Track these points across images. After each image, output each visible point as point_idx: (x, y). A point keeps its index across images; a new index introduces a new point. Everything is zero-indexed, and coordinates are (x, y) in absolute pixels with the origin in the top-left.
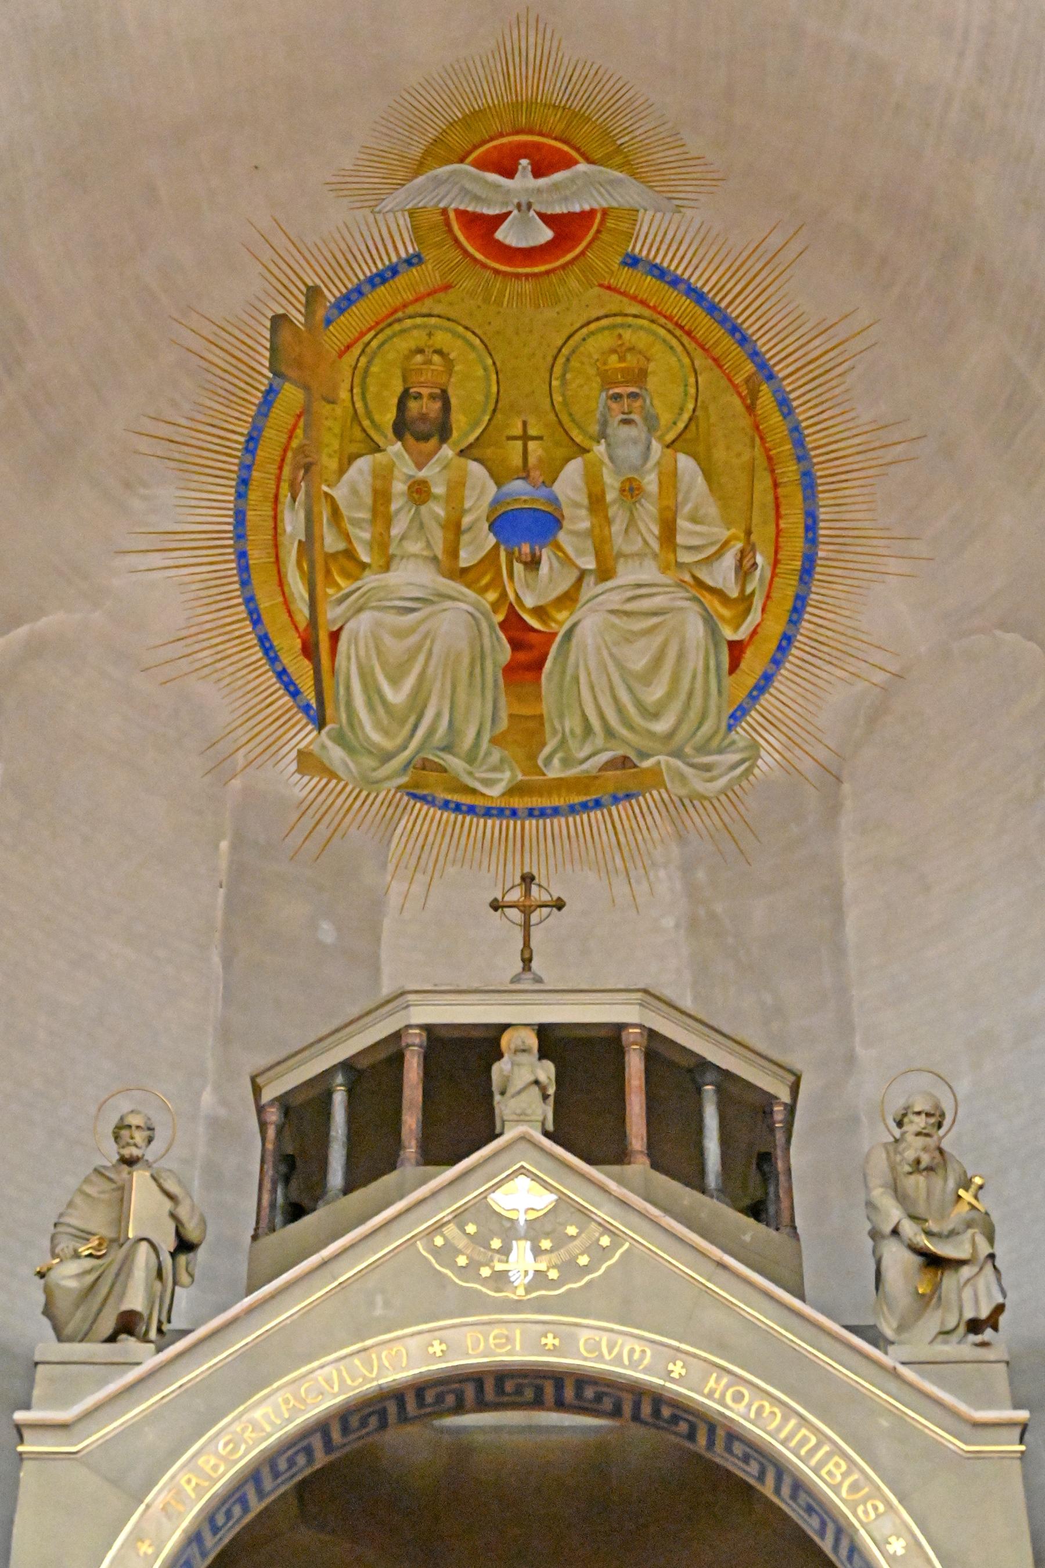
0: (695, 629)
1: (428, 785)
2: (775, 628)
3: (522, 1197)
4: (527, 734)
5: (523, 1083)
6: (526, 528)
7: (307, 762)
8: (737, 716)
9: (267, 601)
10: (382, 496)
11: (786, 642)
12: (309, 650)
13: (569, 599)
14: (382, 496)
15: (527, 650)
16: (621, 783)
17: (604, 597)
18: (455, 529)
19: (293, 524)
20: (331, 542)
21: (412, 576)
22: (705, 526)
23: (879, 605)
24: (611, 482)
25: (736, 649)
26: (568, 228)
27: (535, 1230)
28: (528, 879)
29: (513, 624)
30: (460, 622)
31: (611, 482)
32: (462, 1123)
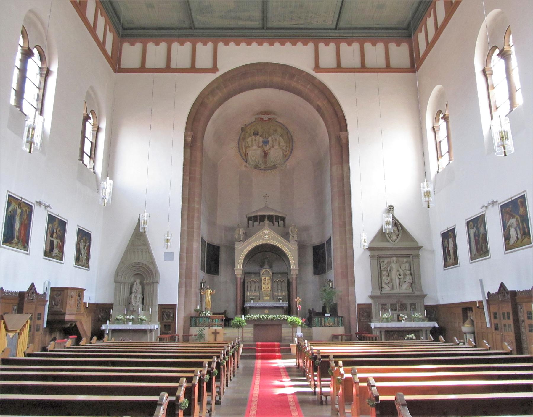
0: (282, 153)
2: (289, 154)
3: (266, 231)
4: (265, 162)
5: (266, 221)
6: (266, 143)
7: (245, 166)
8: (285, 162)
9: (241, 151)
10: (252, 140)
11: (290, 156)
12: (245, 155)
13: (270, 149)
14: (252, 140)
15: (266, 154)
17: (273, 149)
18: (259, 143)
19: (243, 144)
20: (247, 145)
21: (255, 147)
22: (283, 143)
23: (298, 154)
24: (274, 139)
25: (285, 156)
27: (267, 234)
28: (266, 196)
30: (259, 152)
31: (274, 139)
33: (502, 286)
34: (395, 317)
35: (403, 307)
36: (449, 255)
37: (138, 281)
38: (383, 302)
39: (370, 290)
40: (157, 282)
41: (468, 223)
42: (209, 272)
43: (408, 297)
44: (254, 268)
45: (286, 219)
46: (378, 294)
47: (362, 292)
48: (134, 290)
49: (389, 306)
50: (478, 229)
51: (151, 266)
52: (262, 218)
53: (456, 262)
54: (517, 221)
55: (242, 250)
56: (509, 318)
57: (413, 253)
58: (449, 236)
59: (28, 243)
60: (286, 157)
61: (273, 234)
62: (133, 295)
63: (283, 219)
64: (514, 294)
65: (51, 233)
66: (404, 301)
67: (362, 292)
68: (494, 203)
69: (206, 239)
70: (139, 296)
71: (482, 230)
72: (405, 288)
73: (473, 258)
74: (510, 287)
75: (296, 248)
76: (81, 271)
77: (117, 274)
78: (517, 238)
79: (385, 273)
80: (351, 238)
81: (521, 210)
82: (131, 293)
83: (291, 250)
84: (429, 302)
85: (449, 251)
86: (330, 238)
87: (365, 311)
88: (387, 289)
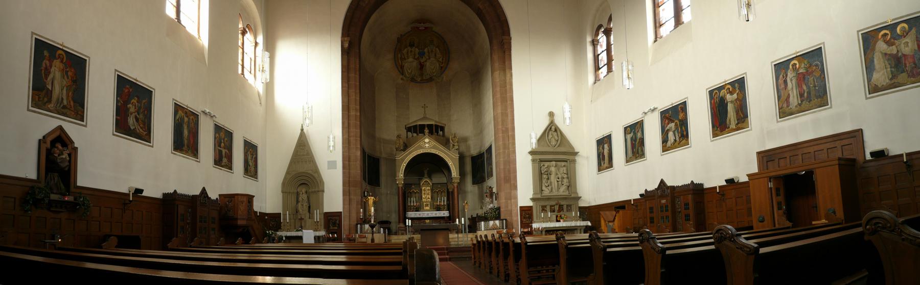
1: (413, 80)
3: (427, 140)
4: (422, 75)
5: (427, 131)
6: (422, 54)
16: (431, 80)
21: (411, 59)
26: (426, 28)
29: (420, 64)
30: (415, 63)
32: (422, 132)
33: (662, 182)
34: (554, 217)
35: (561, 208)
36: (604, 159)
37: (304, 191)
38: (543, 203)
39: (532, 193)
40: (323, 191)
41: (626, 128)
42: (370, 183)
43: (565, 198)
44: (413, 179)
45: (446, 130)
46: (539, 196)
47: (525, 195)
48: (300, 199)
49: (548, 208)
50: (635, 134)
51: (316, 175)
52: (422, 127)
53: (610, 165)
54: (676, 125)
55: (403, 160)
56: (667, 210)
57: (571, 157)
58: (604, 143)
59: (197, 151)
60: (443, 69)
61: (434, 143)
62: (300, 204)
63: (442, 129)
64: (673, 188)
65: (218, 143)
66: (562, 203)
67: (525, 195)
68: (655, 109)
69: (366, 150)
70: (306, 204)
71: (639, 135)
72: (563, 191)
73: (628, 161)
74: (669, 184)
75: (456, 156)
76: (250, 181)
77: (284, 184)
78: (675, 140)
79: (545, 176)
80: (514, 144)
81: (681, 116)
82: (298, 202)
83: (452, 159)
84: (582, 204)
85: (604, 156)
86: (490, 147)
87: (527, 213)
88: (546, 192)
